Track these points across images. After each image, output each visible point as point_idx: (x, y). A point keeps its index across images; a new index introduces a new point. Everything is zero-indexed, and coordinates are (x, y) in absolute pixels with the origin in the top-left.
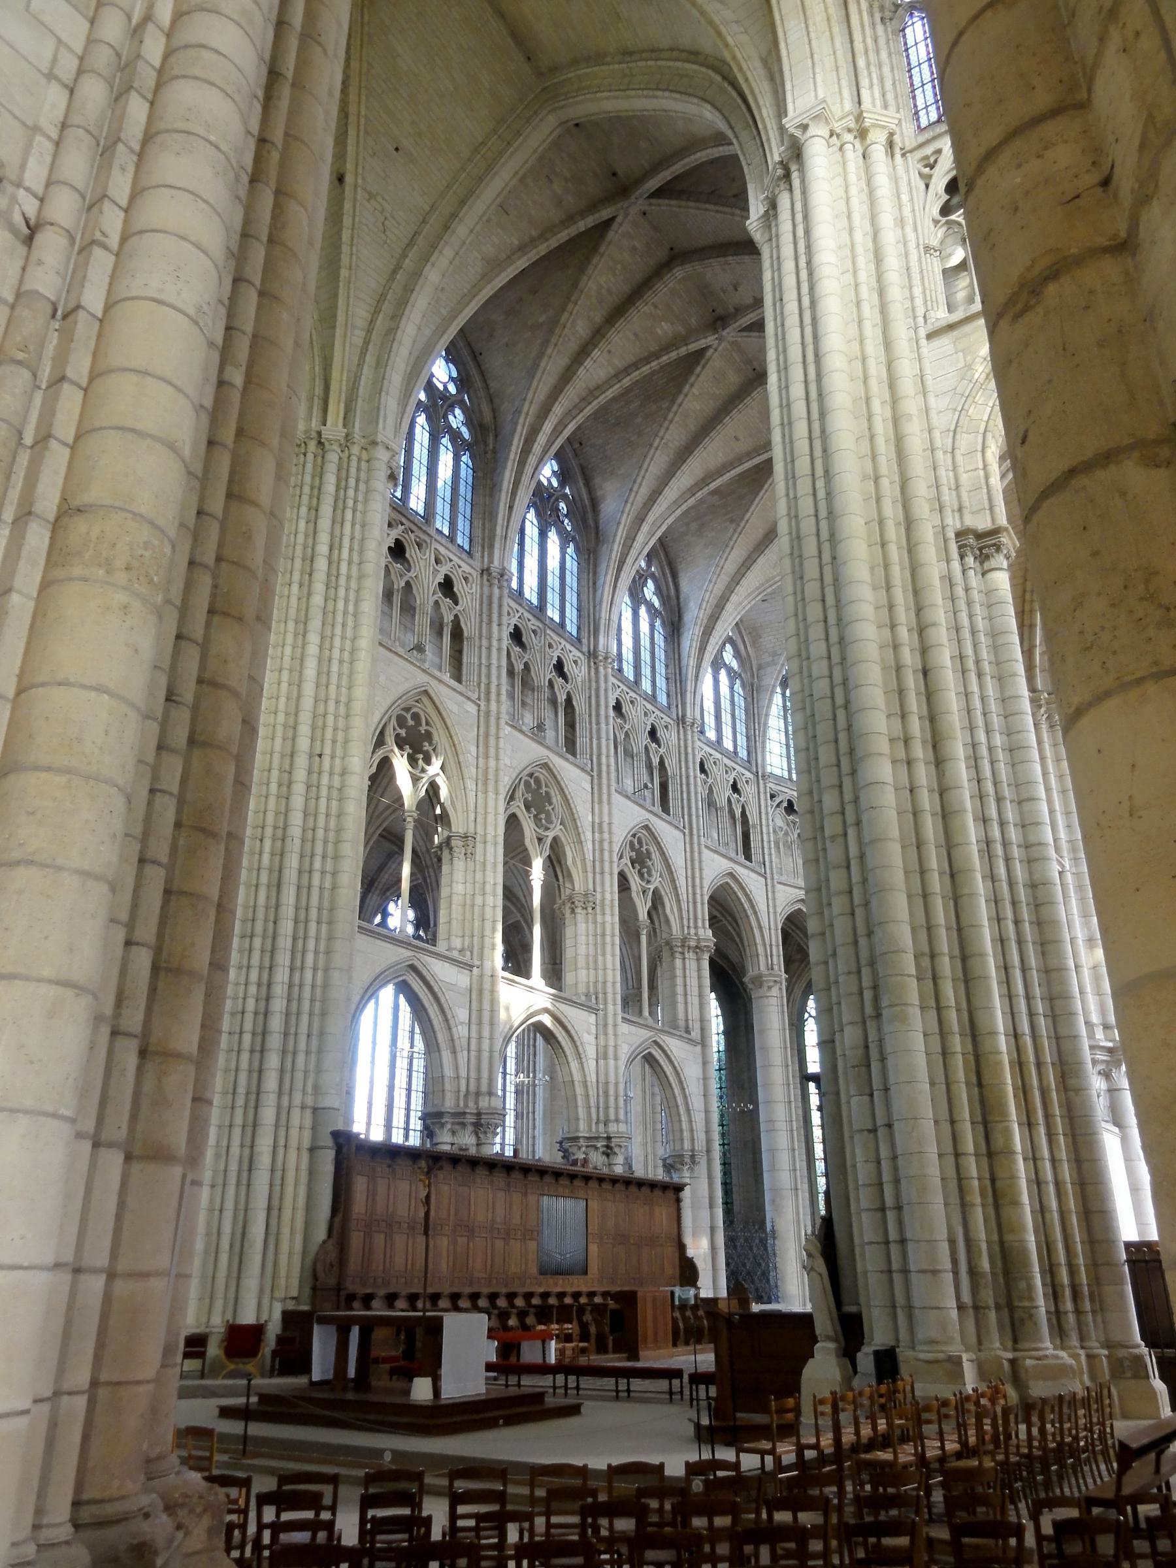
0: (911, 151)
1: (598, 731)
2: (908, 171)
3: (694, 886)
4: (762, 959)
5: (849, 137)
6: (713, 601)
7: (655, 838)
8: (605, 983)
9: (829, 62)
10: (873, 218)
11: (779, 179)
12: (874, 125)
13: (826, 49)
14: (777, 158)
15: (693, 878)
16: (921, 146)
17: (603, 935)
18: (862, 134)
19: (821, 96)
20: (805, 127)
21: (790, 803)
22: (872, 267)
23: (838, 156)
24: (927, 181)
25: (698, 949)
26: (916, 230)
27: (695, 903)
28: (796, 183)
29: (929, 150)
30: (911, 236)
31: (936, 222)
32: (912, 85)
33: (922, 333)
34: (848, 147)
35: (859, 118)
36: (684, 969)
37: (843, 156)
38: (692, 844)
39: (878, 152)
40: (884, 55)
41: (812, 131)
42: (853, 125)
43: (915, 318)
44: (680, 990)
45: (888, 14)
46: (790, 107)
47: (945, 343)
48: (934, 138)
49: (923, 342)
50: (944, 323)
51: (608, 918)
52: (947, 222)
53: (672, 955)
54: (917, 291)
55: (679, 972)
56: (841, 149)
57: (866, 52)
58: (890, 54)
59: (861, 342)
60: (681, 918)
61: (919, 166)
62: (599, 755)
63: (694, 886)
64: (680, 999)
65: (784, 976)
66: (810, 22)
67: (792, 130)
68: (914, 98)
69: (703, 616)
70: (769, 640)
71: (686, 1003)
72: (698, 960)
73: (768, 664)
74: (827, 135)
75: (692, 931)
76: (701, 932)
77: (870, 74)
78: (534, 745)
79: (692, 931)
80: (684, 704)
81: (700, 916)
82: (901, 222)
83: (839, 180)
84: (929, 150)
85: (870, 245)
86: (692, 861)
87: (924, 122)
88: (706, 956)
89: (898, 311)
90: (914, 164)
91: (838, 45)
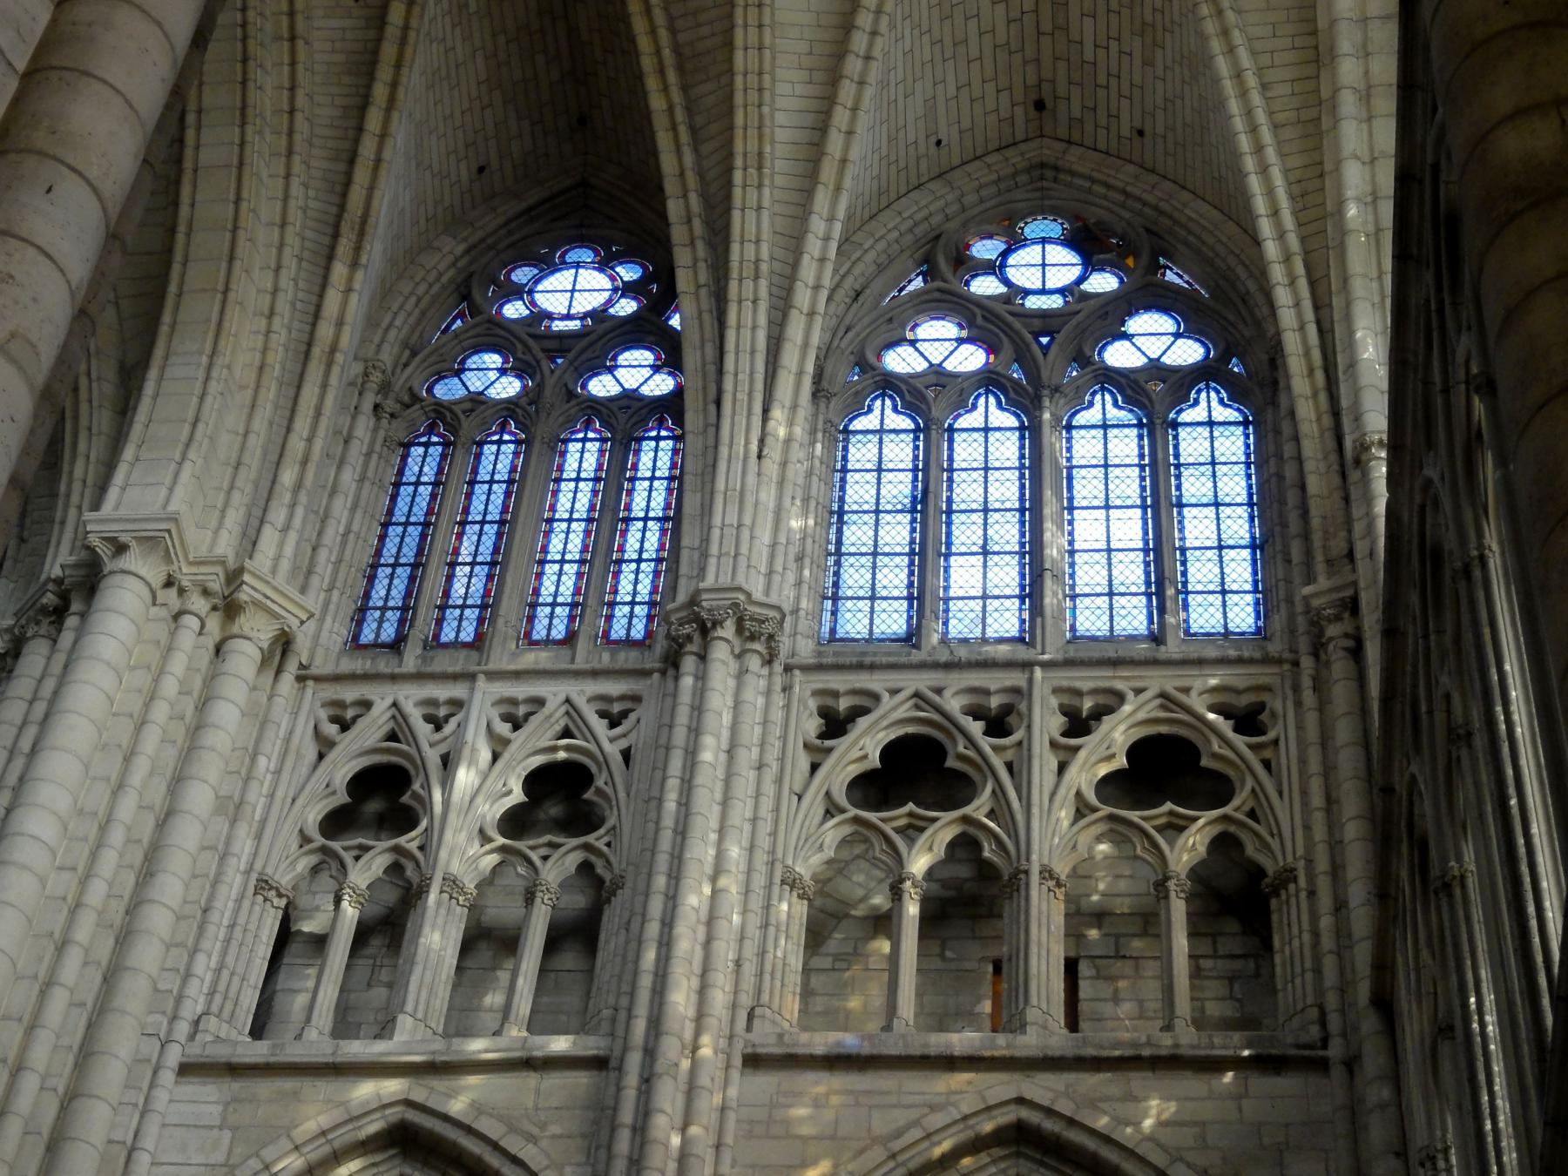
0: (318, 679)
2: (295, 714)
5: (200, 604)
9: (227, 444)
10: (178, 781)
11: (44, 610)
12: (256, 603)
13: (234, 420)
14: (57, 572)
16: (337, 678)
18: (230, 609)
19: (172, 508)
20: (120, 549)
22: (130, 879)
23: (161, 631)
24: (325, 746)
26: (259, 837)
28: (67, 638)
29: (350, 693)
30: (244, 845)
31: (305, 839)
32: (378, 553)
33: (174, 1056)
34: (192, 622)
35: (234, 577)
37: (173, 634)
39: (245, 658)
40: (348, 477)
41: (131, 561)
42: (216, 585)
43: (174, 1018)
45: (390, 405)
46: (113, 494)
47: (208, 1096)
48: (366, 677)
49: (168, 1076)
50: (222, 1053)
52: (324, 850)
54: (203, 966)
56: (176, 617)
57: (305, 462)
58: (362, 479)
59: (31, 1029)
61: (323, 714)
66: (220, 361)
67: (94, 540)
68: (371, 579)
74: (157, 579)
77: (293, 506)
82: (231, 808)
83: (143, 679)
84: (350, 693)
85: (146, 831)
87: (368, 635)
89: (134, 995)
90: (313, 705)
91: (259, 424)
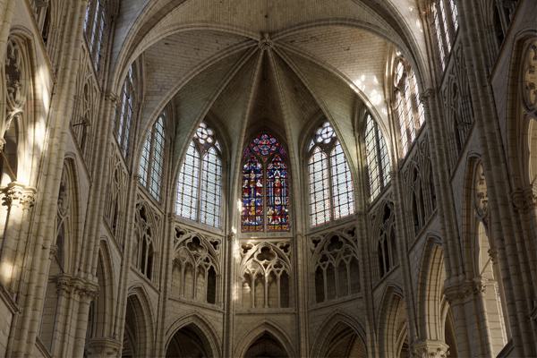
1: (68, 48)
3: (90, 235)
4: (107, 327)
6: (152, 13)
7: (75, 176)
8: (29, 283)
15: (91, 228)
17: (37, 235)
21: (143, 209)
25: (84, 292)
27: (88, 250)
36: (67, 308)
38: (95, 198)
44: (59, 327)
51: (44, 219)
53: (58, 294)
55: (62, 310)
60: (75, 260)
62: (65, 69)
63: (90, 235)
64: (58, 335)
65: (122, 347)
69: (144, 18)
70: (160, 76)
71: (63, 341)
72: (81, 303)
73: (156, 93)
75: (82, 275)
76: (90, 277)
78: (28, 15)
79: (82, 275)
80: (110, 81)
81: (91, 263)
86: (93, 212)
88: (89, 301)
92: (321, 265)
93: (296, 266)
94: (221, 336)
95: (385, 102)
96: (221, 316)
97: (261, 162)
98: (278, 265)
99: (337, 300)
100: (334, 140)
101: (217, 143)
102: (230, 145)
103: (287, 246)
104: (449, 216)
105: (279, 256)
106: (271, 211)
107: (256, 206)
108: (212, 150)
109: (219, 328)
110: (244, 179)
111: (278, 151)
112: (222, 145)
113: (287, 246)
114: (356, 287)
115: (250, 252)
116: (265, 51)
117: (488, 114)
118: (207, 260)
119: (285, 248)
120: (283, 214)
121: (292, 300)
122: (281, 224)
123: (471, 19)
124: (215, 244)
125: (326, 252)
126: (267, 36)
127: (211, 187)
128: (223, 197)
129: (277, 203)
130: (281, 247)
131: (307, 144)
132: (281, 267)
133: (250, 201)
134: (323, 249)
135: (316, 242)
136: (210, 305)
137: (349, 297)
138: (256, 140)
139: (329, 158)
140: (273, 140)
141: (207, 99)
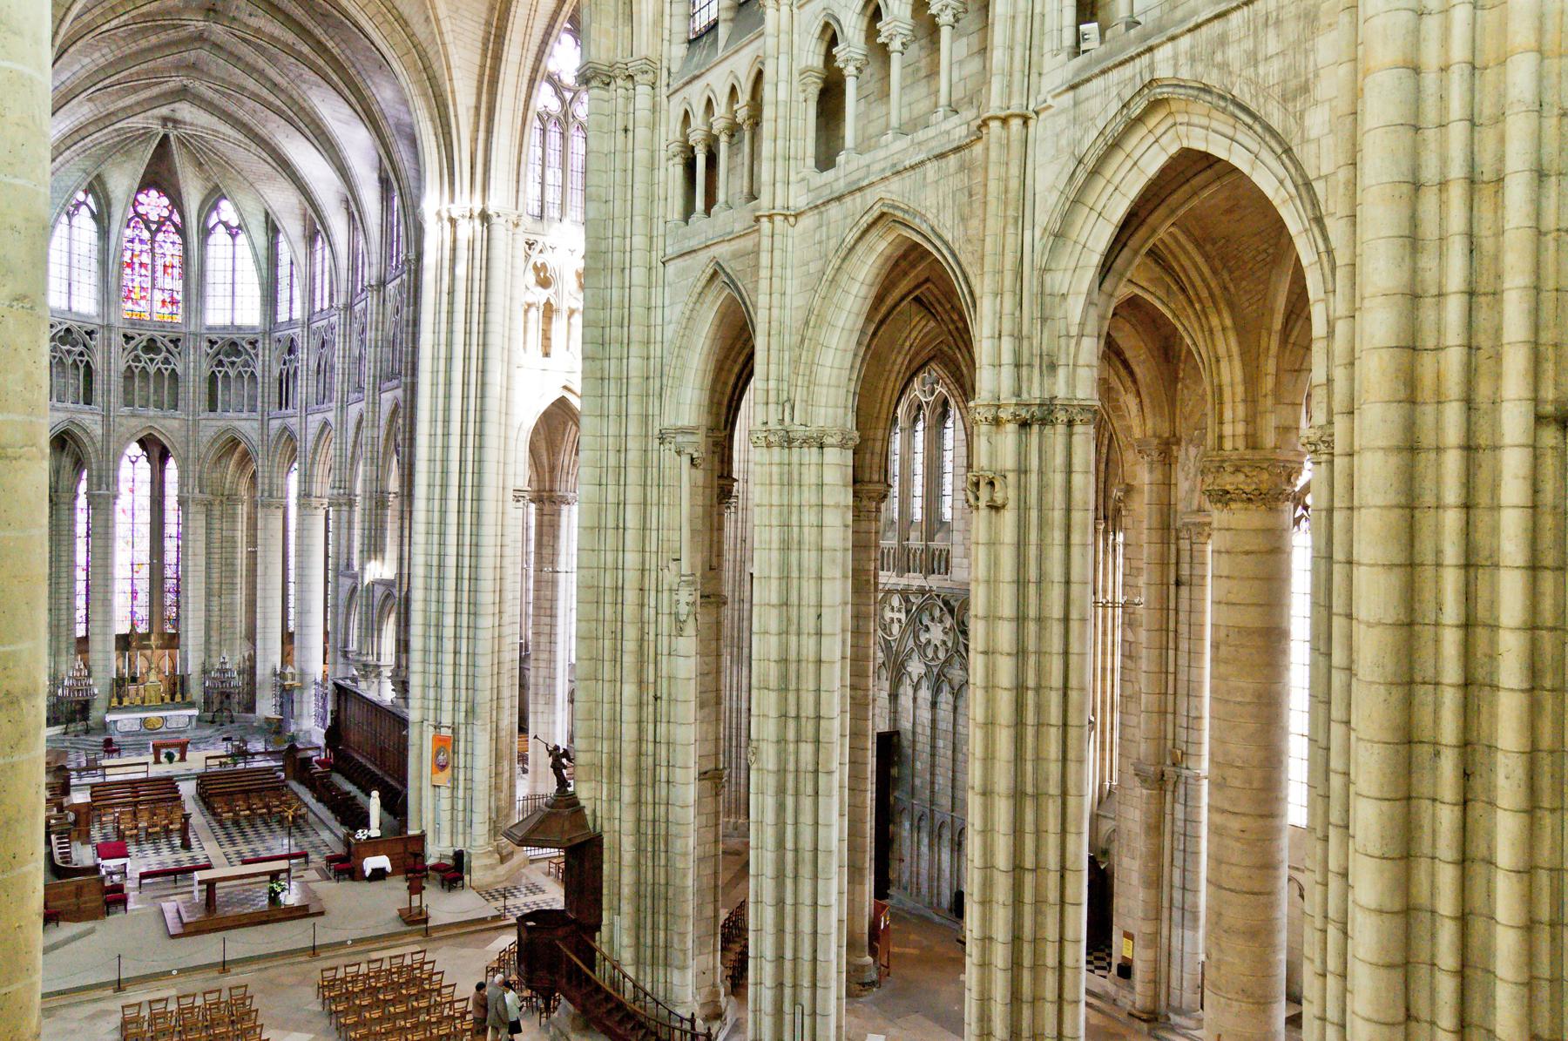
92: (216, 369)
93: (187, 368)
94: (100, 438)
95: (304, 236)
96: (99, 418)
97: (148, 228)
98: (166, 361)
99: (231, 414)
100: (239, 227)
101: (91, 200)
102: (109, 205)
103: (178, 340)
104: (341, 434)
105: (168, 351)
106: (158, 296)
107: (142, 288)
108: (84, 210)
109: (98, 430)
110: (127, 249)
111: (169, 218)
112: (98, 203)
113: (178, 340)
114: (253, 398)
115: (133, 343)
116: (166, 137)
117: (373, 421)
118: (81, 354)
119: (175, 342)
120: (174, 302)
121: (181, 404)
122: (172, 313)
123: (377, 322)
124: (90, 333)
125: (221, 357)
126: (170, 125)
127: (84, 263)
128: (100, 273)
129: (167, 287)
130: (171, 341)
131: (208, 216)
132: (170, 363)
133: (133, 280)
134: (218, 354)
135: (212, 343)
136: (87, 407)
137: (244, 415)
138: (141, 198)
139: (234, 245)
140: (165, 201)
141: (84, 171)
